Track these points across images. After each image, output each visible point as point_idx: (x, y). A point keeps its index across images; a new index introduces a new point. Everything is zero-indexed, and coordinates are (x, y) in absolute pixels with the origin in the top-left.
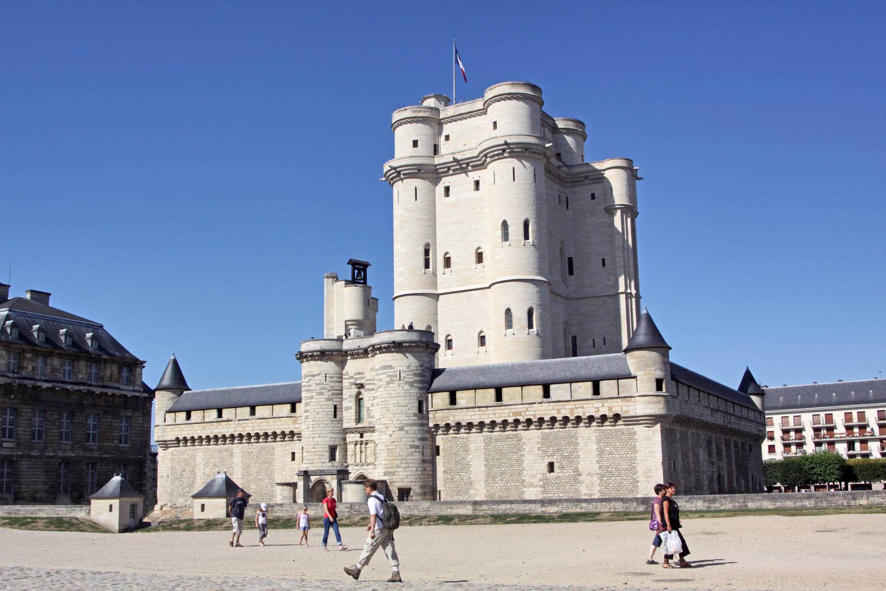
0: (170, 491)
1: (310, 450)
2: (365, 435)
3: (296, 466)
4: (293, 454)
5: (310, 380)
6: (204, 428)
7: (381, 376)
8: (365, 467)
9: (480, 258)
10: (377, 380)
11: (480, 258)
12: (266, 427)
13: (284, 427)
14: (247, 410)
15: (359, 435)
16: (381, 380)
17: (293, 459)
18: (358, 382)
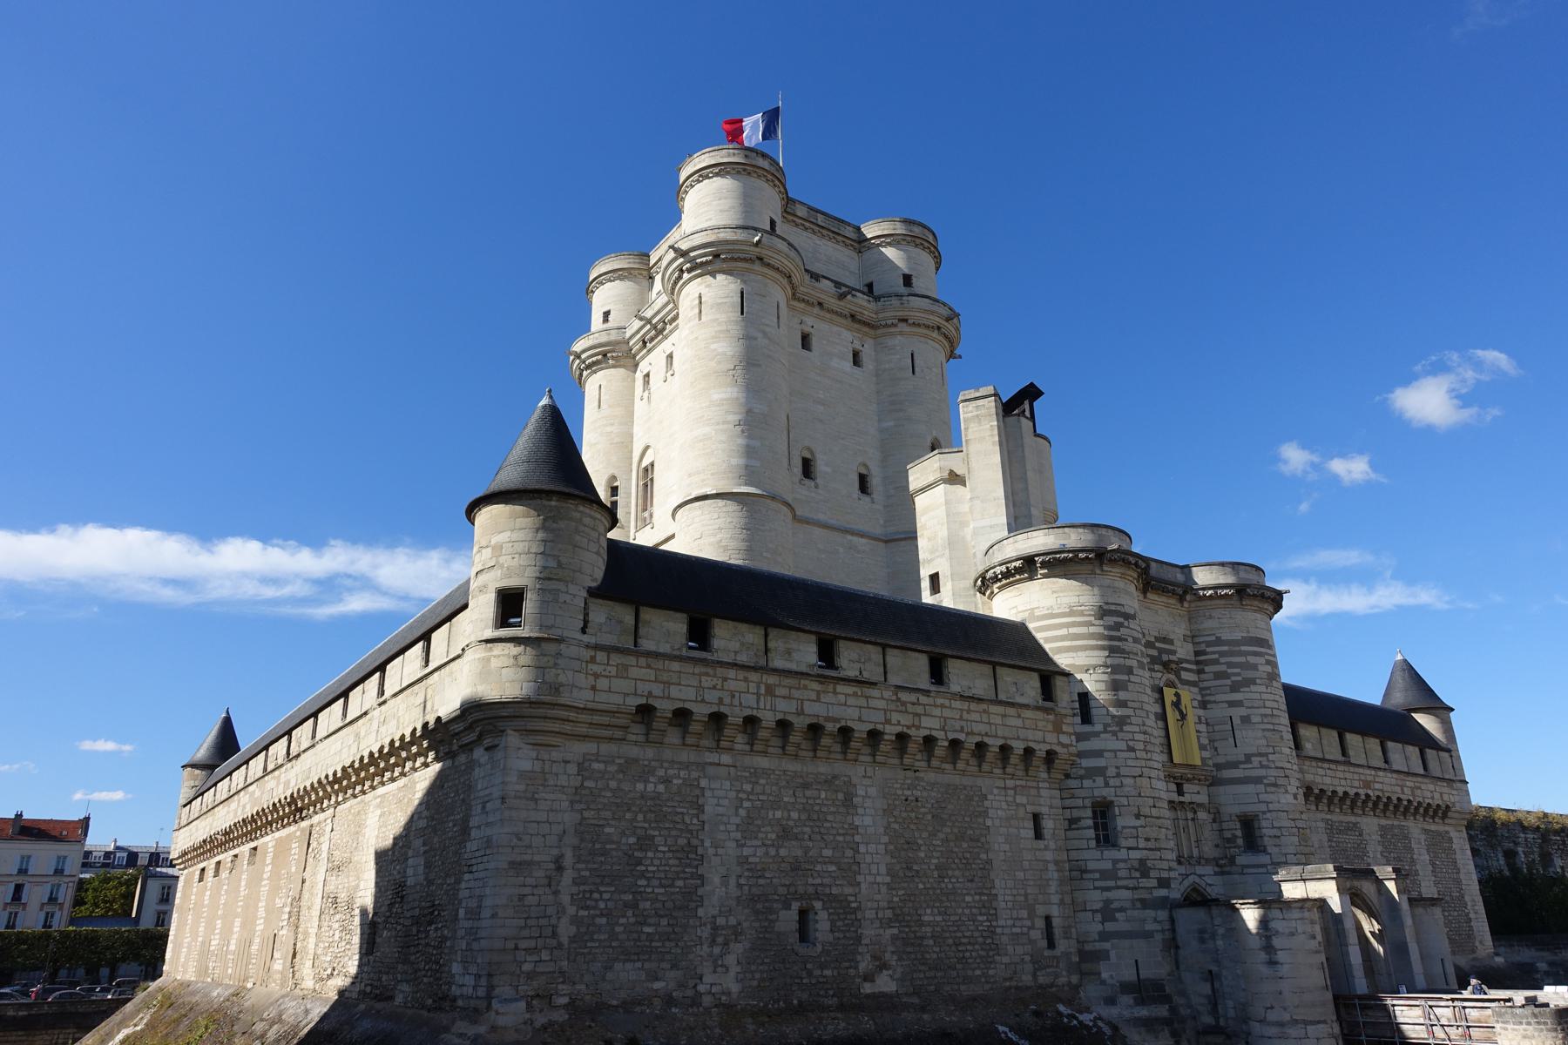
0: (566, 930)
1: (1145, 811)
2: (1186, 787)
3: (1049, 856)
4: (1036, 818)
5: (1118, 626)
6: (770, 691)
7: (1252, 659)
8: (1200, 870)
9: (864, 484)
10: (1230, 665)
11: (864, 484)
12: (982, 728)
13: (1030, 735)
14: (921, 663)
15: (1173, 787)
16: (1255, 667)
17: (1038, 835)
18: (1165, 658)
